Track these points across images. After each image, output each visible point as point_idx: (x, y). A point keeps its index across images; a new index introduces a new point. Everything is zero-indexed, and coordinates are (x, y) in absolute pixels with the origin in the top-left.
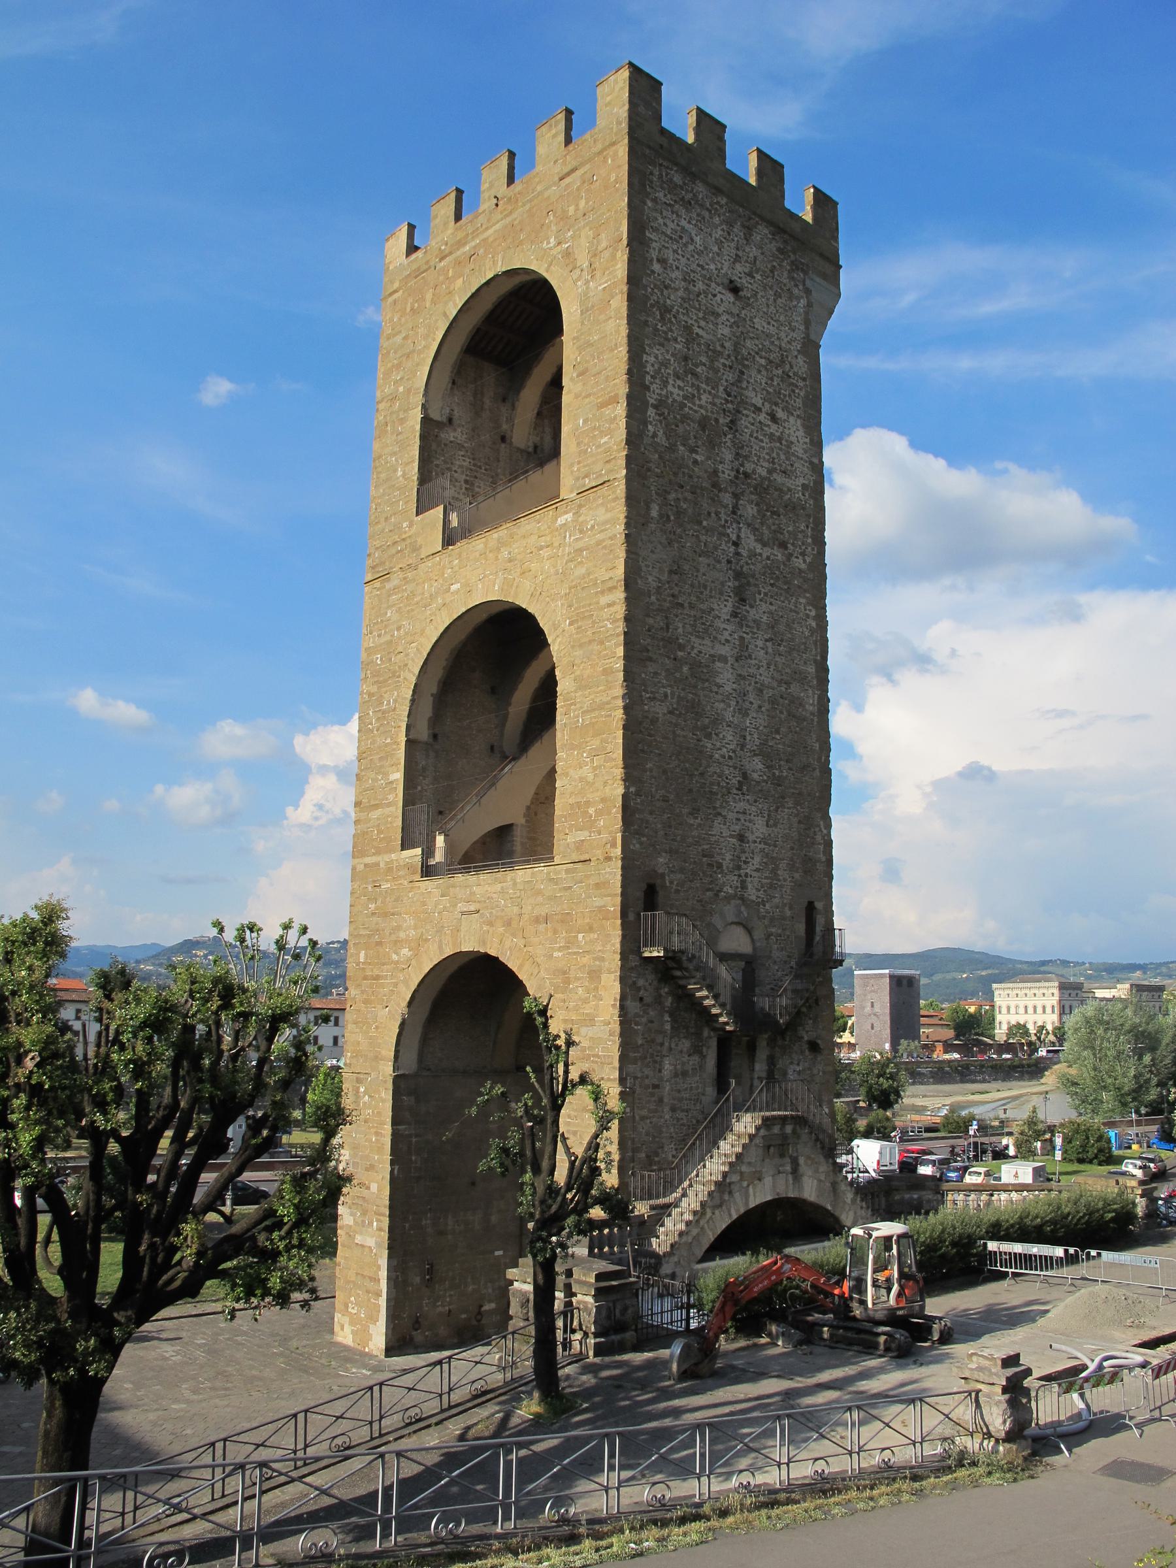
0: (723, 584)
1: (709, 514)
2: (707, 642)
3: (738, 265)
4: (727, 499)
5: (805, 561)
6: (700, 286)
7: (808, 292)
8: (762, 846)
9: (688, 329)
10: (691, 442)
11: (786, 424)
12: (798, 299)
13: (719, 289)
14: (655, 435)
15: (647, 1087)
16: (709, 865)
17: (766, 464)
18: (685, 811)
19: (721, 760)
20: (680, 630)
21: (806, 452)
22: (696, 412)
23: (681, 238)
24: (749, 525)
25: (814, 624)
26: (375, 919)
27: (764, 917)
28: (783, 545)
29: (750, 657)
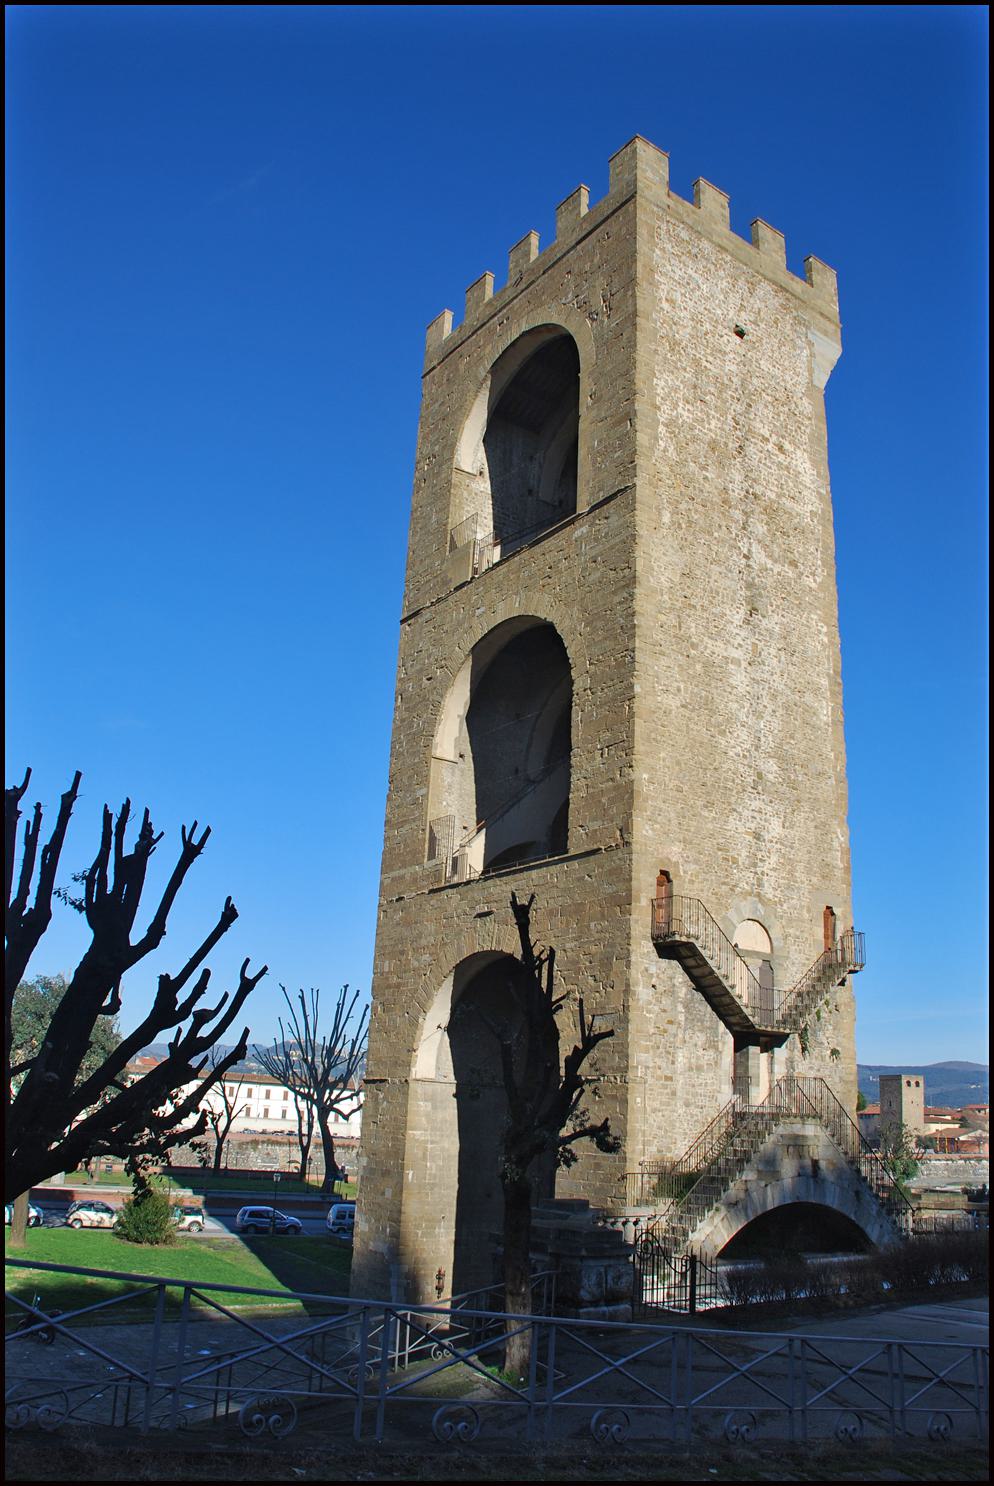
0: (735, 593)
1: (720, 526)
3: (743, 313)
4: (737, 514)
5: (815, 581)
6: (707, 326)
7: (811, 344)
8: (779, 846)
9: (696, 362)
11: (794, 456)
12: (802, 349)
13: (726, 331)
14: (665, 450)
15: (659, 1078)
16: (724, 859)
17: (775, 489)
18: (700, 803)
19: (736, 758)
20: (693, 630)
21: (813, 483)
22: (706, 434)
23: (688, 284)
24: (759, 542)
25: (826, 640)
26: (399, 929)
27: (782, 917)
28: (793, 564)
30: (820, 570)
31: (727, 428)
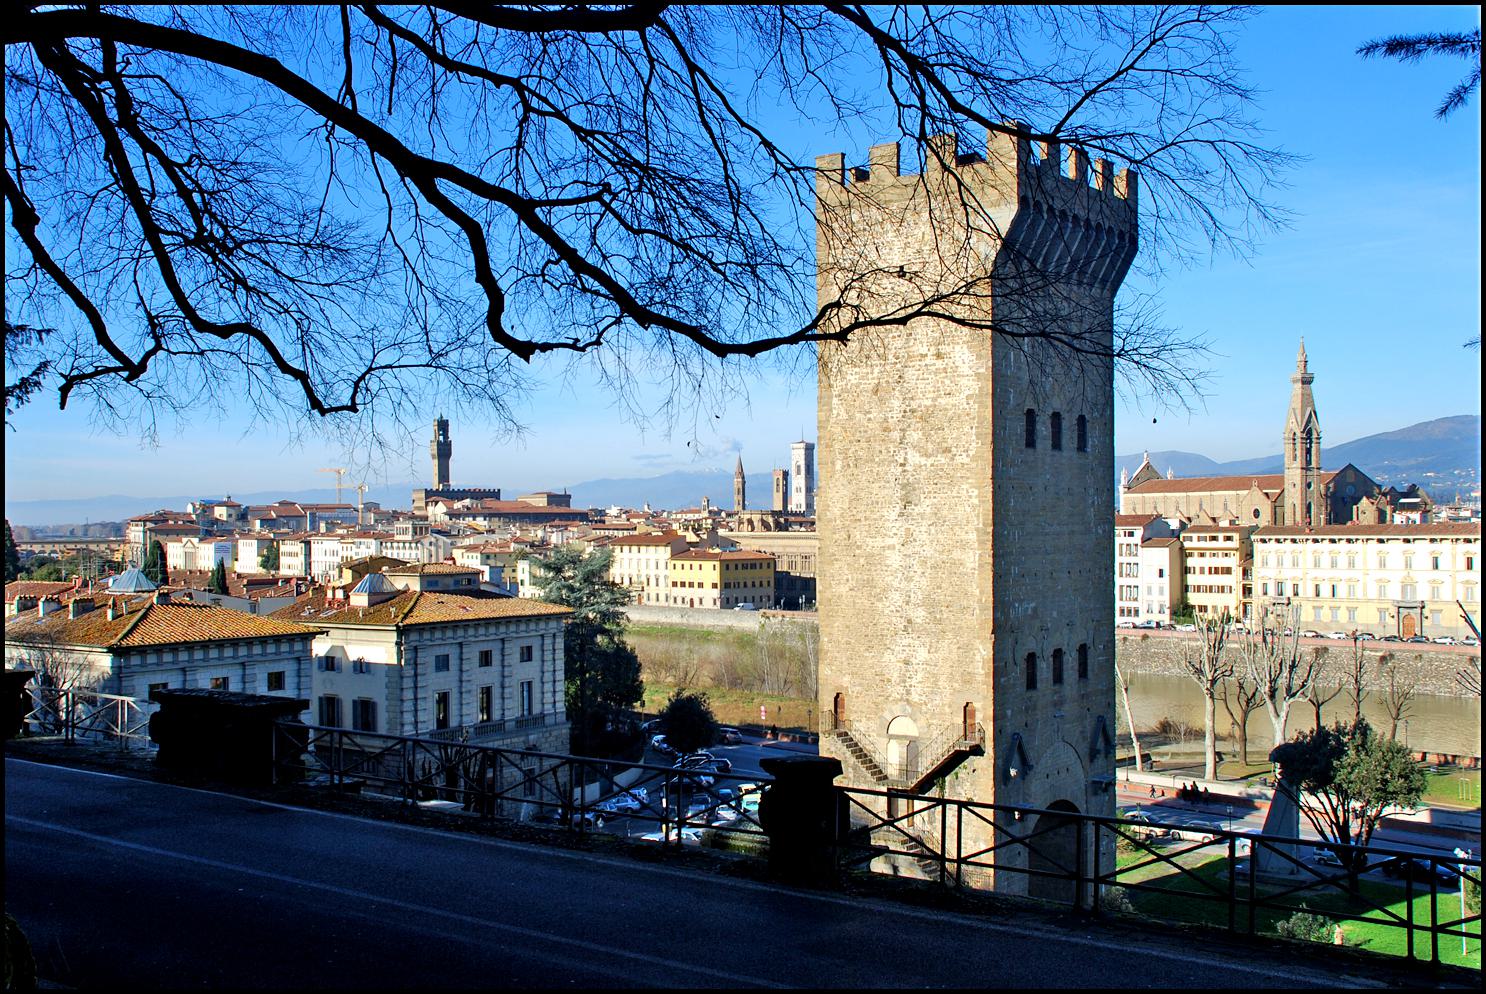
2: (879, 539)
10: (867, 407)
14: (838, 414)
25: (976, 501)
28: (947, 450)
29: (915, 540)
30: (974, 444)
31: (888, 368)
